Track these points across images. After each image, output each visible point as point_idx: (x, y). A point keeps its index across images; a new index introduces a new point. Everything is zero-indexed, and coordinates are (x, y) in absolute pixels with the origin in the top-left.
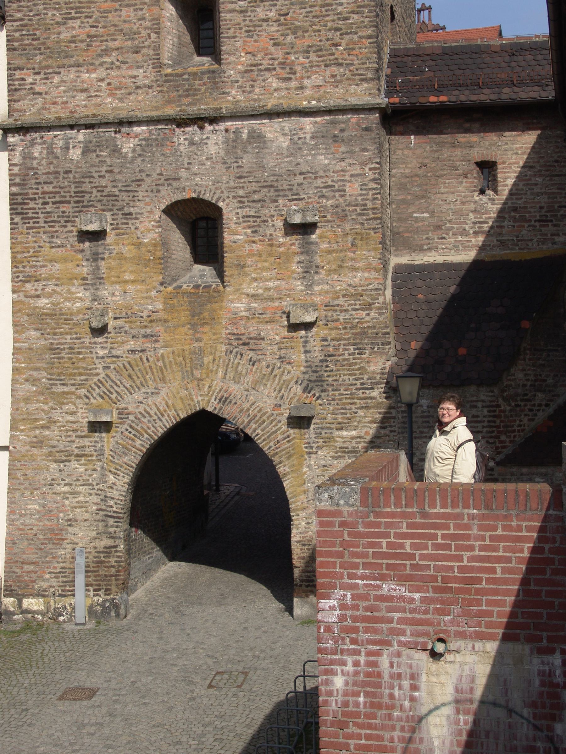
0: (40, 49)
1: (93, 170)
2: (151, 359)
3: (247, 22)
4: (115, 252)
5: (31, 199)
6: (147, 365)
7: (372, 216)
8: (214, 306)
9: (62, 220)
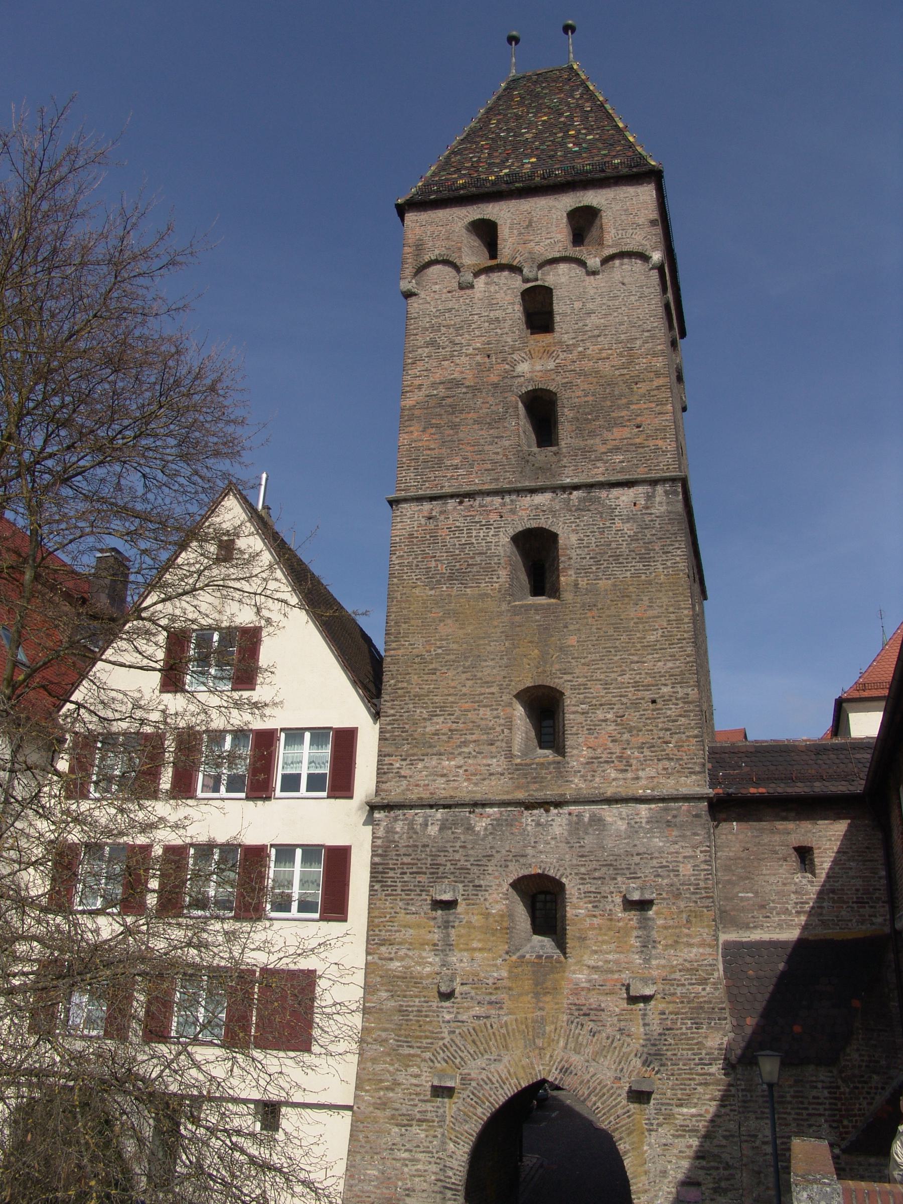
0: (407, 740)
1: (448, 845)
2: (495, 1026)
3: (588, 722)
4: (465, 921)
5: (391, 869)
6: (491, 1031)
7: (705, 895)
8: (557, 976)
9: (418, 889)
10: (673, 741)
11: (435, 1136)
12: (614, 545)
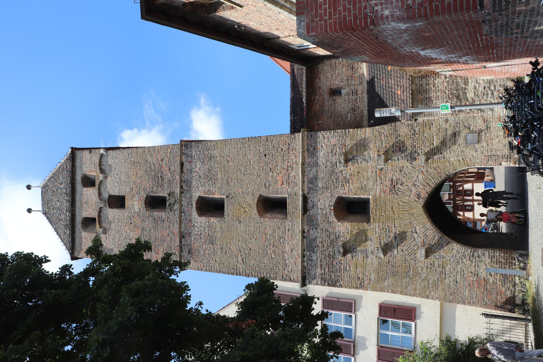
10: (281, 146)
11: (450, 260)
12: (205, 172)
